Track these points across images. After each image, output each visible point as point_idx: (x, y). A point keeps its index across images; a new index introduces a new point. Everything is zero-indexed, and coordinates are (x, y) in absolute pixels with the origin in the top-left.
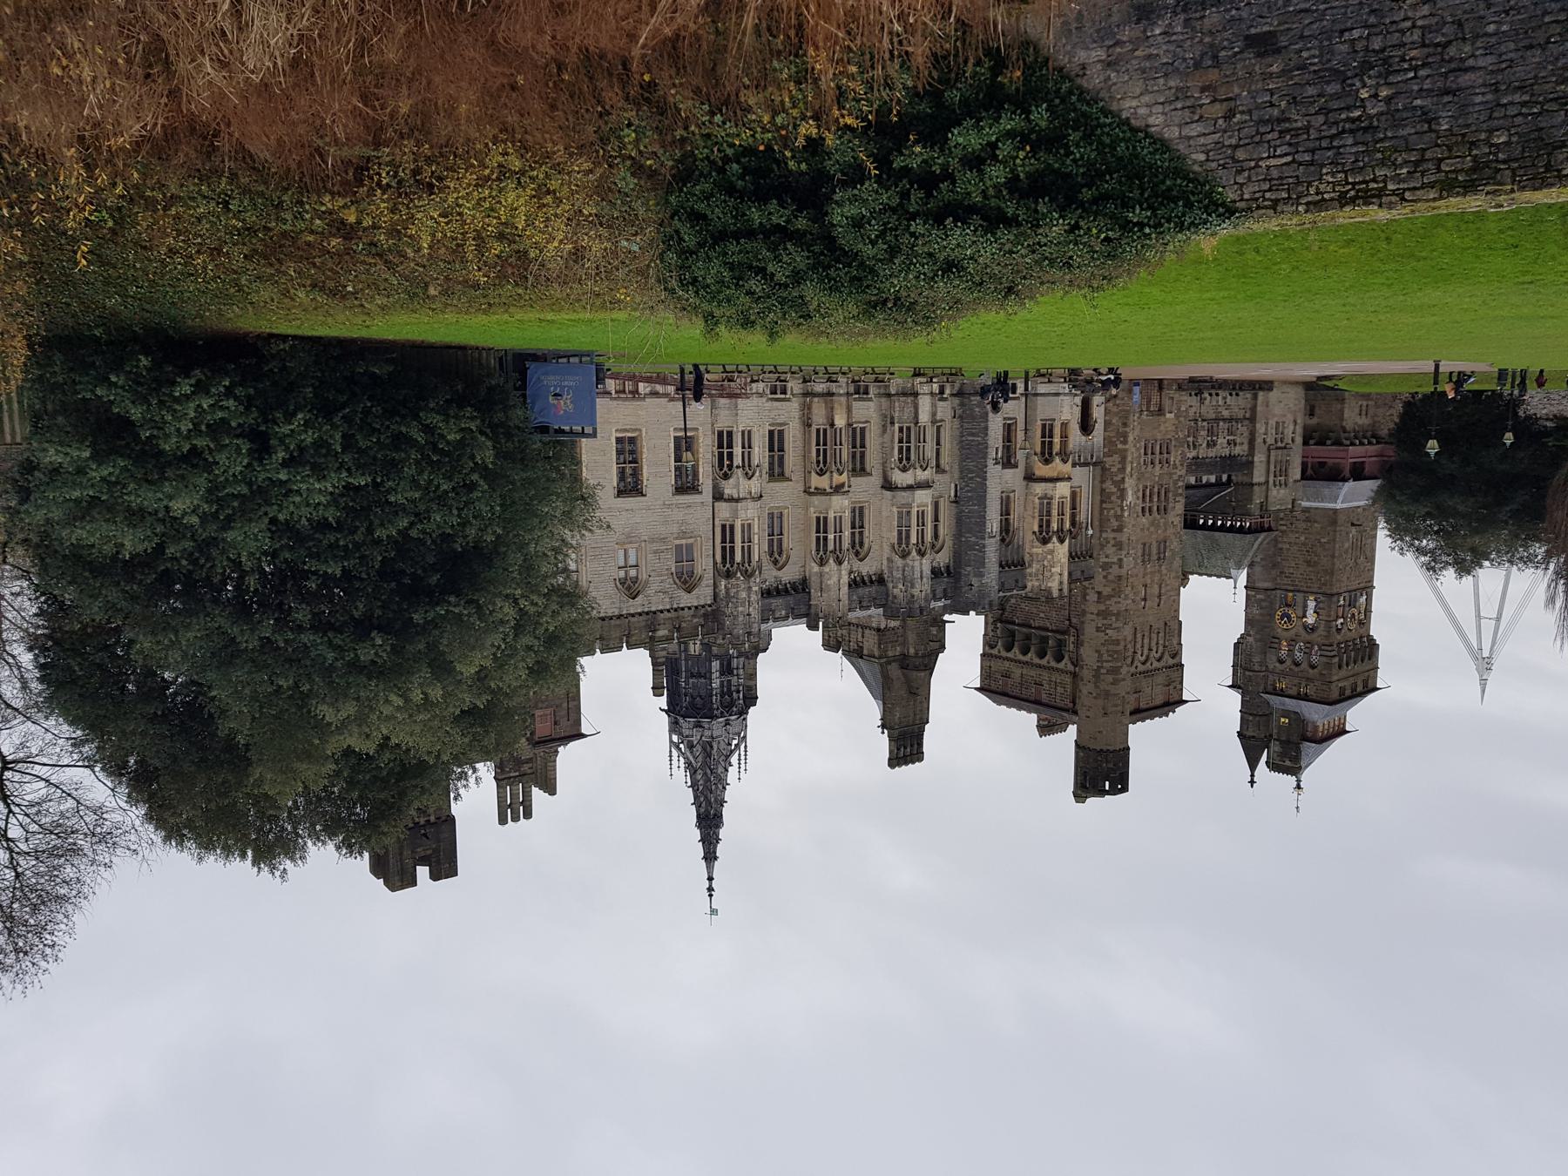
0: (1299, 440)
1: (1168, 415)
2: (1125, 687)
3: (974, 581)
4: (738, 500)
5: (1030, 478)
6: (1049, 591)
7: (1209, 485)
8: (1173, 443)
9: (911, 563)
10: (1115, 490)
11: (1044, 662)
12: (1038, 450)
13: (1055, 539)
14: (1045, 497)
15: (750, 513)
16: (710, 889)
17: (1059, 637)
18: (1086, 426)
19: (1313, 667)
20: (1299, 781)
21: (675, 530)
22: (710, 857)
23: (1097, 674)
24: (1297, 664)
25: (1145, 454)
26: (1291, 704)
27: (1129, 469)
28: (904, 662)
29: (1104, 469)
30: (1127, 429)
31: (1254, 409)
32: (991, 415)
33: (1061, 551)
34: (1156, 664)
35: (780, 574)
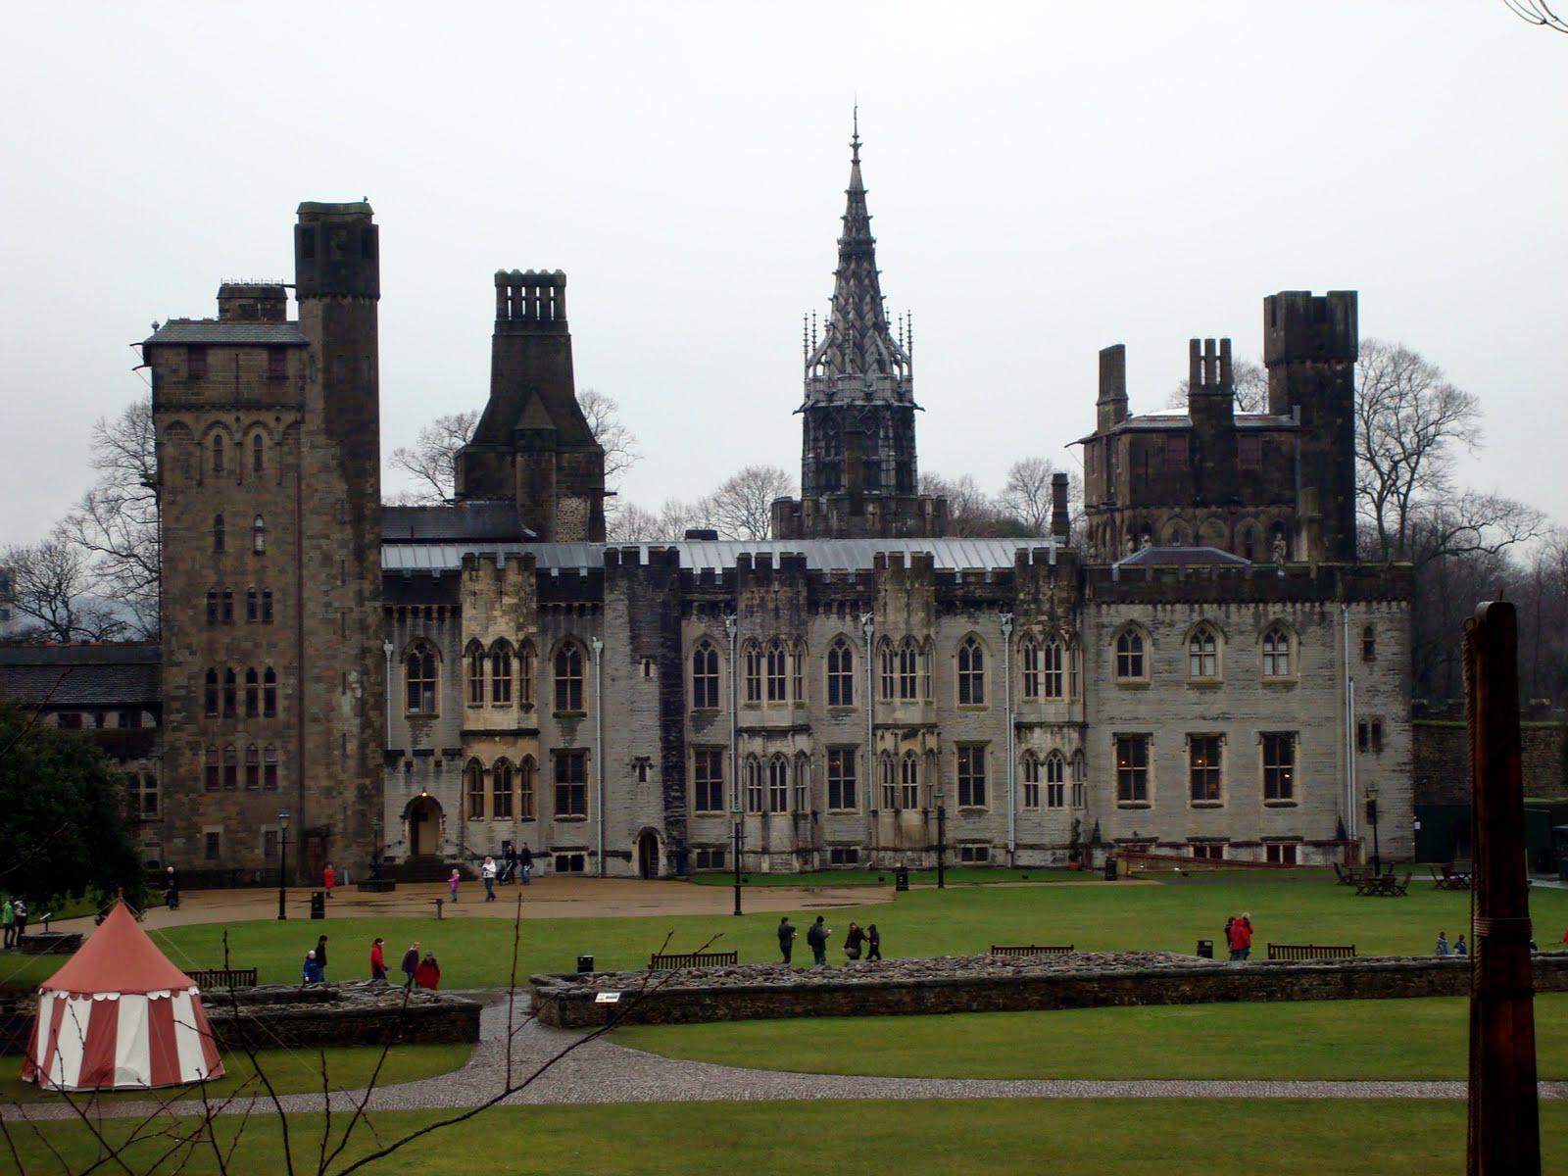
1: (219, 829)
4: (1071, 724)
8: (201, 785)
9: (794, 632)
12: (536, 779)
13: (516, 646)
15: (1052, 709)
16: (856, 147)
18: (422, 812)
21: (1150, 695)
22: (856, 195)
25: (271, 770)
27: (352, 747)
29: (382, 744)
30: (359, 807)
32: (659, 825)
34: (228, 418)
35: (970, 627)
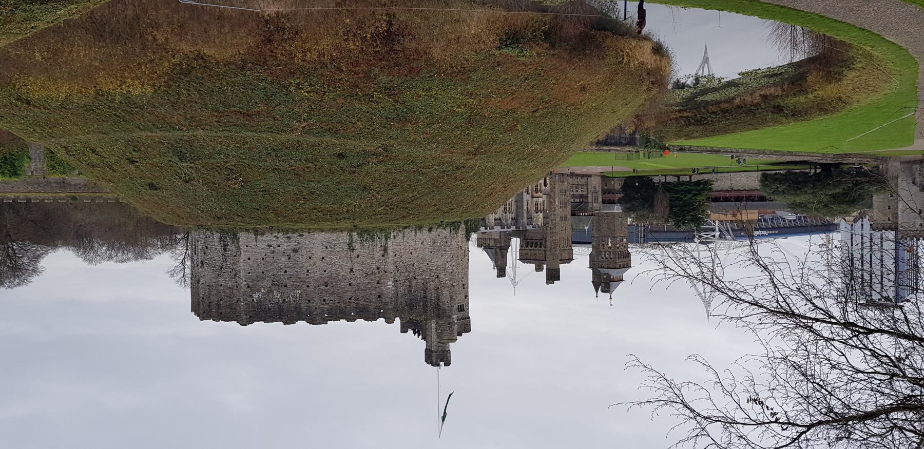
0: (600, 191)
2: (558, 252)
3: (521, 221)
5: (533, 197)
6: (538, 225)
7: (577, 202)
10: (553, 201)
11: (537, 249)
14: (536, 201)
17: (541, 241)
18: (545, 185)
19: (611, 259)
20: (611, 296)
23: (551, 249)
24: (607, 258)
26: (606, 271)
28: (501, 248)
31: (587, 183)
33: (541, 215)
34: (566, 248)
